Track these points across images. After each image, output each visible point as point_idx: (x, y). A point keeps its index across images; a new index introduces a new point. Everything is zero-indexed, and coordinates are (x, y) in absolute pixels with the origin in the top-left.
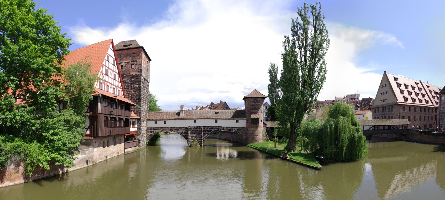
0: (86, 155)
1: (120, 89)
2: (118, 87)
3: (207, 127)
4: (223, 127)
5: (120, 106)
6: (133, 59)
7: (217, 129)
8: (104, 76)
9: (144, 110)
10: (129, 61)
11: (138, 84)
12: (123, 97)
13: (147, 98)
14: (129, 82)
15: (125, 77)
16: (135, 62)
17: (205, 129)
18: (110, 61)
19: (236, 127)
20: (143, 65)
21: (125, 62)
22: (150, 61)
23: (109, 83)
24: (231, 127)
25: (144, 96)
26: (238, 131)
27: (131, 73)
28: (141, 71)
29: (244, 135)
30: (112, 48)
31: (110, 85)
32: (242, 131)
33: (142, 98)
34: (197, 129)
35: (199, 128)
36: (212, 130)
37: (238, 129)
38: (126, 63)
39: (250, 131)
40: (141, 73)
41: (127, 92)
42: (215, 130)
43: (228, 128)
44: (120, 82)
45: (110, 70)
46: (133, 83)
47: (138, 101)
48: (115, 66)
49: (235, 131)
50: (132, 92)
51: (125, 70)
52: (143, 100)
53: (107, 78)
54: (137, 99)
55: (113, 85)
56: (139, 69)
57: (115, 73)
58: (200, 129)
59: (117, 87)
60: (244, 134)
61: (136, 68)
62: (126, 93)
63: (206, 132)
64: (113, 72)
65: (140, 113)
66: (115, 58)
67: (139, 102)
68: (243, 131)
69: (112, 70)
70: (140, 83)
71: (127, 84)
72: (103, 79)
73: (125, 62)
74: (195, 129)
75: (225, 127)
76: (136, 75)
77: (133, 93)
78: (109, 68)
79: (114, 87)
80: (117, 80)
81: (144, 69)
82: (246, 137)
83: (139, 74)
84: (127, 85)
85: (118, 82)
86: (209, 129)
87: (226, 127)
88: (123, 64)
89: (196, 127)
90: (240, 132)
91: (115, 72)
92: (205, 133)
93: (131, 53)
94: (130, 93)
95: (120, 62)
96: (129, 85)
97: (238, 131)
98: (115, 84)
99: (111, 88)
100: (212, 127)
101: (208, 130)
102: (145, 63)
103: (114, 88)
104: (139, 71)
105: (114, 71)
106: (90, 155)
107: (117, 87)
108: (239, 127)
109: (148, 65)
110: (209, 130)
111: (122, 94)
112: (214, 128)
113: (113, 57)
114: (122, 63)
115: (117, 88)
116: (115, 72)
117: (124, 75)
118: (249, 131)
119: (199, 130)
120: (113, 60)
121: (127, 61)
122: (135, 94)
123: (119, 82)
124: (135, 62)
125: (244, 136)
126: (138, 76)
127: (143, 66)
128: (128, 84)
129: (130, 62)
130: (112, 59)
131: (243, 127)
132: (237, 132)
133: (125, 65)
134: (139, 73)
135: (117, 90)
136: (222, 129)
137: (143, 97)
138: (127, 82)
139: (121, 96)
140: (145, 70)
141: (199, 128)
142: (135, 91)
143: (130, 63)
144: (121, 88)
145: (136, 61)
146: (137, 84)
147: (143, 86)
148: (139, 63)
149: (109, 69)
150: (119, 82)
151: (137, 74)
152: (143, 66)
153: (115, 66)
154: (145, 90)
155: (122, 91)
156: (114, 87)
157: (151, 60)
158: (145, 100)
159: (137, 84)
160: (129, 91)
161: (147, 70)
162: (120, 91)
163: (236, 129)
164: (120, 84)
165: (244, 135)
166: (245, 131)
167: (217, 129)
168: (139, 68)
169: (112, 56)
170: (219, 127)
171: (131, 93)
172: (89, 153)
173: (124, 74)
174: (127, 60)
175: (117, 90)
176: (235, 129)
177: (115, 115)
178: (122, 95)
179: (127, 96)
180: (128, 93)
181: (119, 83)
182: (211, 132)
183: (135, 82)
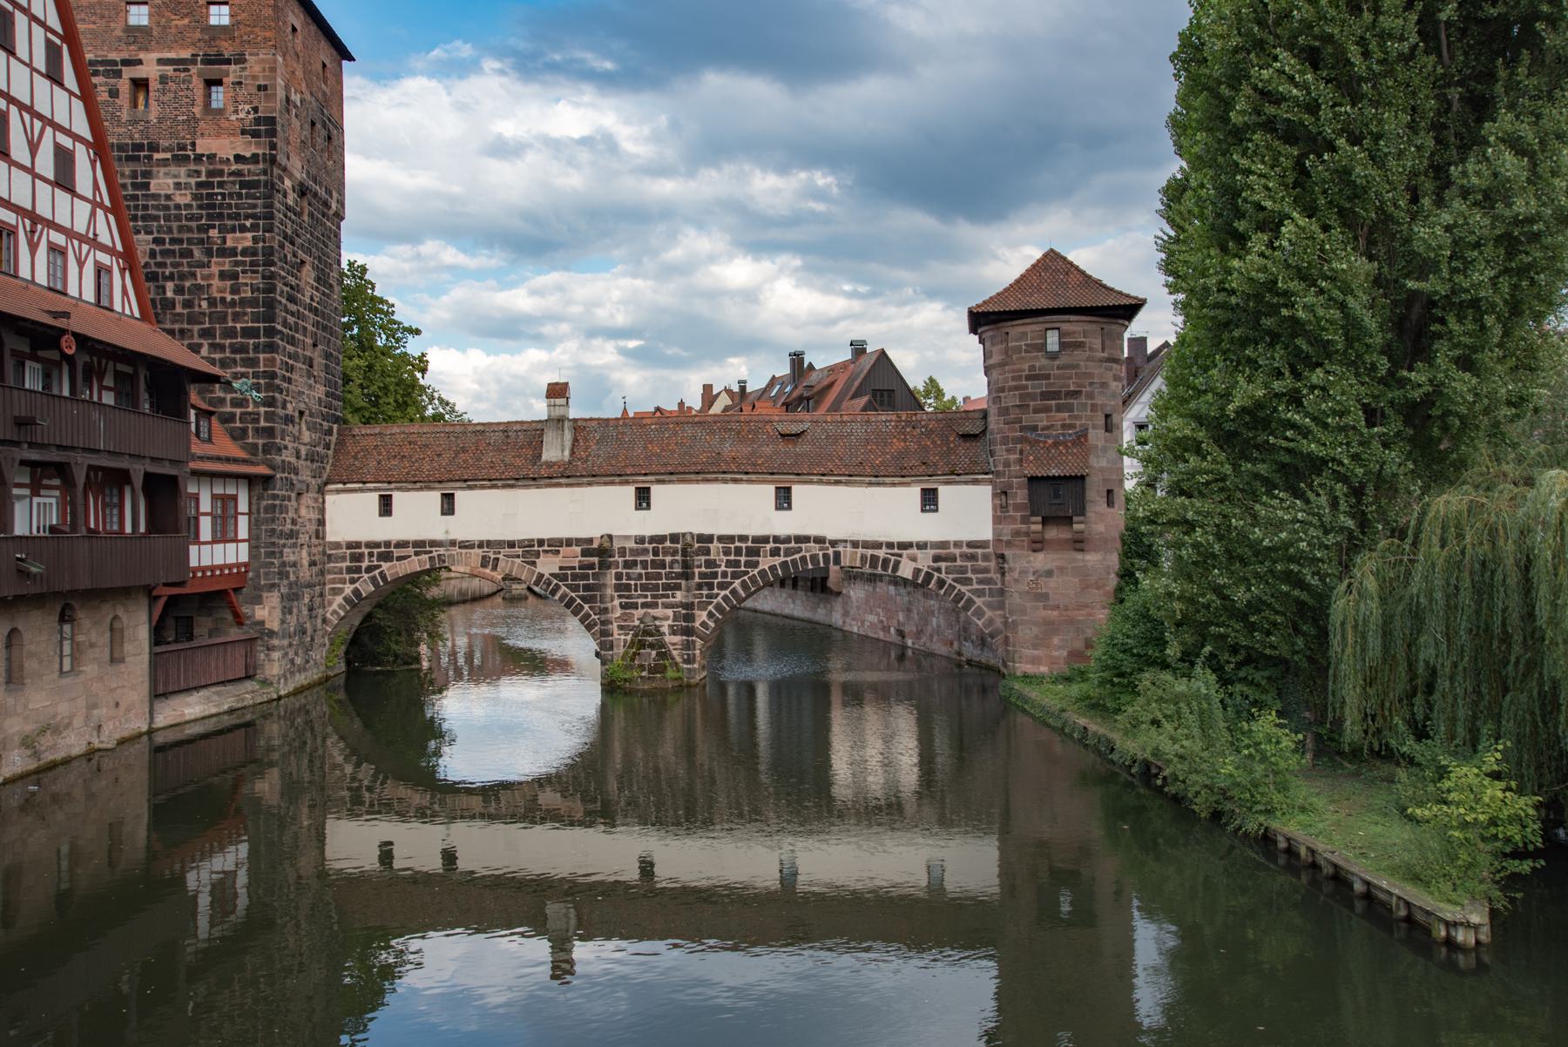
1: (105, 258)
2: (94, 243)
3: (721, 539)
4: (834, 543)
5: (109, 381)
6: (217, 43)
7: (788, 552)
9: (301, 413)
10: (186, 54)
11: (254, 227)
12: (137, 315)
13: (325, 328)
14: (188, 206)
15: (163, 170)
16: (228, 62)
17: (708, 552)
18: (22, 49)
19: (922, 546)
20: (287, 88)
21: (161, 62)
22: (345, 63)
23: (17, 209)
24: (890, 545)
25: (298, 315)
26: (939, 570)
27: (204, 146)
28: (272, 133)
29: (979, 601)
31: (27, 222)
32: (963, 570)
33: (285, 323)
34: (656, 553)
35: (668, 544)
36: (756, 564)
37: (937, 559)
38: (171, 68)
39: (1023, 572)
40: (273, 146)
41: (182, 277)
42: (777, 561)
43: (870, 552)
44: (107, 203)
45: (27, 117)
46: (220, 216)
47: (256, 348)
48: (61, 85)
49: (917, 571)
50: (216, 282)
51: (160, 120)
52: (292, 341)
54: (249, 333)
55: (52, 225)
56: (258, 121)
57: (66, 142)
58: (675, 553)
59: (82, 239)
60: (980, 593)
61: (236, 112)
62: (170, 286)
63: (715, 575)
64: (49, 130)
65: (270, 432)
66: (60, 30)
67: (261, 356)
68: (975, 571)
69: (40, 117)
70: (270, 216)
71: (178, 218)
73: (161, 62)
74: (646, 551)
75: (846, 541)
76: (239, 158)
77: (220, 284)
79: (59, 239)
80: (79, 190)
81: (296, 123)
82: (999, 623)
83: (260, 152)
84: (175, 225)
85: (88, 206)
86: (738, 551)
87: (855, 544)
88: (149, 69)
89: (653, 539)
90: (954, 580)
91: (68, 132)
92: (711, 586)
94: (199, 288)
95: (125, 55)
96: (190, 230)
97: (939, 570)
98: (63, 219)
99: (33, 248)
100: (757, 540)
101: (729, 564)
102: (299, 73)
103: (53, 248)
104: (255, 134)
105: (57, 127)
107: (82, 239)
108: (944, 545)
109: (327, 91)
110: (737, 564)
111: (125, 292)
112: (768, 547)
113: (43, 24)
114: (140, 62)
115: (85, 247)
116: (68, 132)
117: (156, 156)
118: (1016, 575)
119: (668, 559)
120: (48, 41)
122: (236, 297)
123: (101, 205)
124: (233, 67)
125: (979, 613)
126: (252, 167)
127: (288, 99)
128: (187, 219)
129: (193, 61)
130: (38, 32)
131: (970, 544)
132: (929, 576)
133: (163, 79)
134: (258, 144)
135: (81, 264)
136: (826, 556)
137: (291, 320)
138: (178, 207)
139: (117, 307)
140: (307, 126)
141: (668, 544)
142: (235, 276)
143: (194, 70)
144: (119, 247)
145: (240, 60)
146: (248, 224)
147: (293, 243)
148: (254, 78)
149: (14, 110)
150: (101, 205)
151: (248, 155)
152: (288, 99)
153: (61, 85)
154: (308, 268)
155: (122, 271)
156: (59, 239)
157: (351, 59)
158: (309, 341)
159: (248, 224)
160: (194, 275)
161: (324, 125)
162: (109, 271)
163: (925, 561)
165: (979, 601)
166: (986, 570)
167: (788, 552)
168: (256, 110)
170: (806, 539)
171: (209, 286)
173: (154, 148)
174: (170, 49)
175: (81, 264)
176: (914, 559)
177: (59, 447)
178: (123, 297)
179: (179, 309)
180: (187, 284)
181: (100, 212)
182: (753, 579)
183: (230, 206)
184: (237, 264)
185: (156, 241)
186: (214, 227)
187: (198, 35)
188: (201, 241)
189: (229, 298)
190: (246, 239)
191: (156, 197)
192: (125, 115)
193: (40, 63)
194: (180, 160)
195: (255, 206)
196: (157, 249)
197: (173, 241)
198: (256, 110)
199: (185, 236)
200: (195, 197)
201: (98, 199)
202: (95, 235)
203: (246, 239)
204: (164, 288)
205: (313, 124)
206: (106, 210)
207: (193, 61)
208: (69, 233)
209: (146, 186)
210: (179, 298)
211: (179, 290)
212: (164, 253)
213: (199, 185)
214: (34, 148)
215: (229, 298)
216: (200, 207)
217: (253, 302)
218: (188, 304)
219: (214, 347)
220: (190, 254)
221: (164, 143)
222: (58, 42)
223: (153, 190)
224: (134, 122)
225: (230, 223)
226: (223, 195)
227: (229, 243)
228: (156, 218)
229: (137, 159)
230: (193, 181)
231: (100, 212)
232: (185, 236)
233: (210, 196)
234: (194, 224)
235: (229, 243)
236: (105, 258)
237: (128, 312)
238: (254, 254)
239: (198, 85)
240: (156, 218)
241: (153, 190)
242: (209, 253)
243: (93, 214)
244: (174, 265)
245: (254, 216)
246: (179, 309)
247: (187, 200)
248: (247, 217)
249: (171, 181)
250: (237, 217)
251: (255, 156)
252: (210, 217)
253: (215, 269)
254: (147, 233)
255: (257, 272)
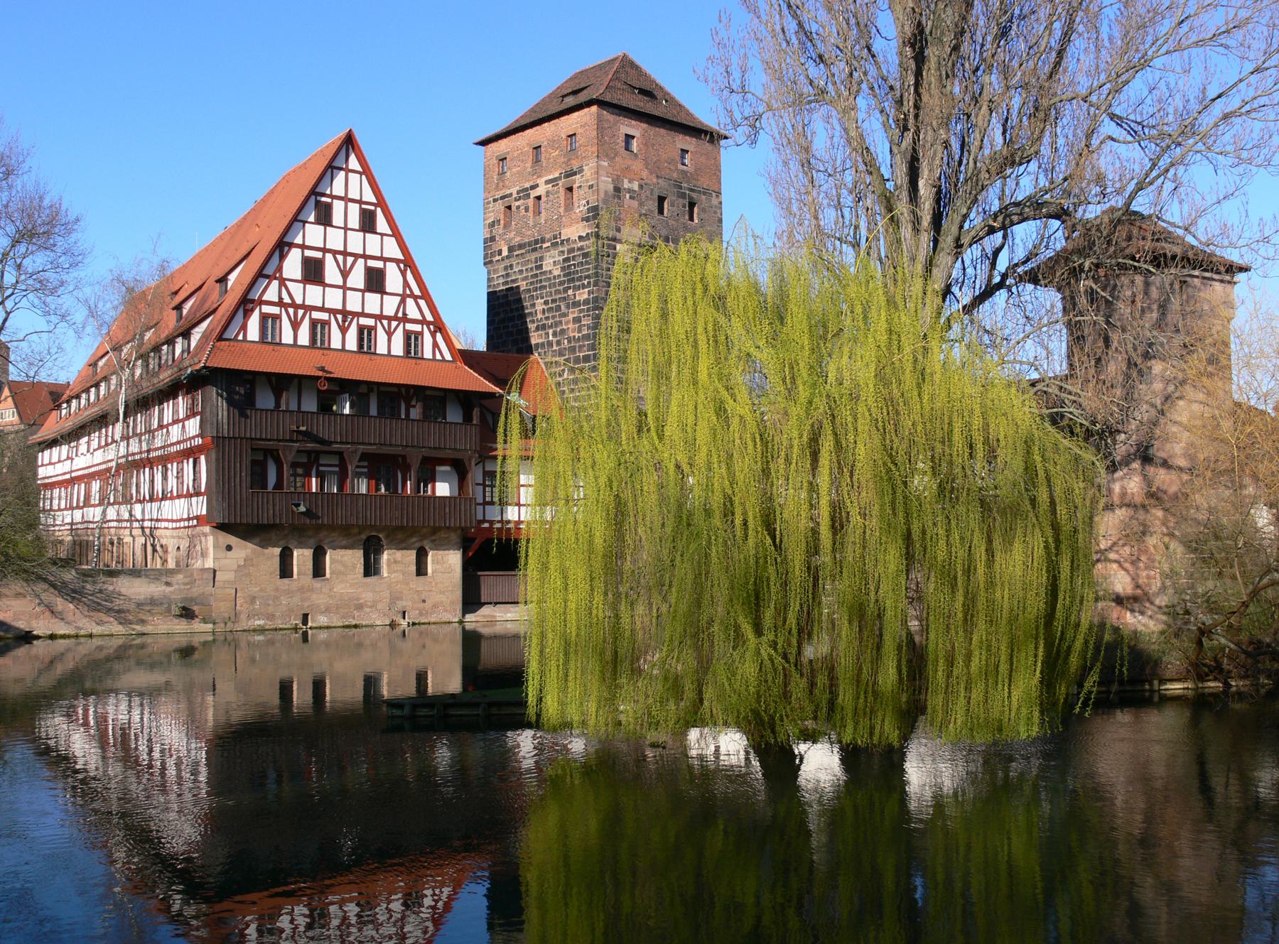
0: (169, 589)
1: (417, 328)
2: (405, 319)
8: (296, 289)
10: (557, 175)
12: (448, 357)
14: (559, 276)
15: (548, 254)
16: (575, 174)
18: (337, 218)
21: (547, 182)
23: (330, 311)
30: (353, 163)
31: (340, 317)
44: (417, 292)
46: (573, 280)
50: (571, 326)
53: (313, 294)
54: (586, 359)
55: (363, 314)
59: (390, 319)
64: (361, 261)
72: (287, 300)
73: (547, 182)
76: (580, 238)
78: (324, 250)
84: (553, 290)
88: (541, 191)
93: (564, 137)
94: (563, 331)
95: (531, 183)
104: (587, 219)
106: (195, 590)
111: (435, 345)
114: (537, 186)
115: (394, 324)
117: (545, 246)
121: (551, 177)
123: (412, 296)
124: (578, 176)
126: (587, 242)
127: (617, 189)
128: (559, 285)
129: (559, 178)
133: (548, 192)
135: (390, 334)
138: (554, 277)
143: (560, 183)
144: (429, 318)
148: (587, 181)
150: (412, 296)
155: (433, 335)
156: (371, 322)
160: (561, 322)
164: (422, 303)
169: (353, 194)
172: (187, 584)
173: (543, 241)
174: (551, 172)
175: (390, 334)
179: (555, 348)
181: (410, 302)
184: (581, 311)
185: (546, 303)
186: (570, 288)
187: (562, 160)
188: (564, 298)
189: (577, 335)
190: (583, 295)
191: (545, 272)
192: (531, 223)
193: (354, 221)
194: (555, 245)
195: (588, 269)
196: (545, 307)
197: (554, 301)
198: (588, 203)
199: (558, 296)
200: (563, 269)
201: (408, 292)
202: (405, 314)
203: (583, 295)
204: (548, 334)
205: (661, 200)
206: (415, 298)
207: (559, 178)
208: (379, 317)
209: (541, 267)
210: (555, 339)
211: (555, 334)
212: (550, 310)
213: (565, 260)
214: (345, 274)
215: (577, 335)
216: (564, 276)
217: (586, 337)
218: (558, 343)
219: (572, 370)
220: (558, 308)
221: (548, 236)
222: (372, 208)
223: (545, 269)
224: (535, 226)
225: (577, 283)
226: (574, 265)
227: (577, 298)
228: (545, 287)
229: (535, 250)
230: (561, 258)
231: (410, 302)
232: (558, 296)
233: (569, 266)
234: (561, 288)
235: (577, 298)
236: (417, 328)
237: (438, 357)
238: (588, 304)
239: (562, 191)
240: (545, 287)
241: (545, 269)
242: (568, 307)
243: (403, 302)
244: (553, 317)
245: (588, 277)
246: (555, 348)
247: (556, 273)
248: (586, 277)
249: (551, 261)
250: (580, 279)
251: (588, 234)
252: (569, 281)
253: (571, 317)
254: (542, 298)
255: (589, 316)
